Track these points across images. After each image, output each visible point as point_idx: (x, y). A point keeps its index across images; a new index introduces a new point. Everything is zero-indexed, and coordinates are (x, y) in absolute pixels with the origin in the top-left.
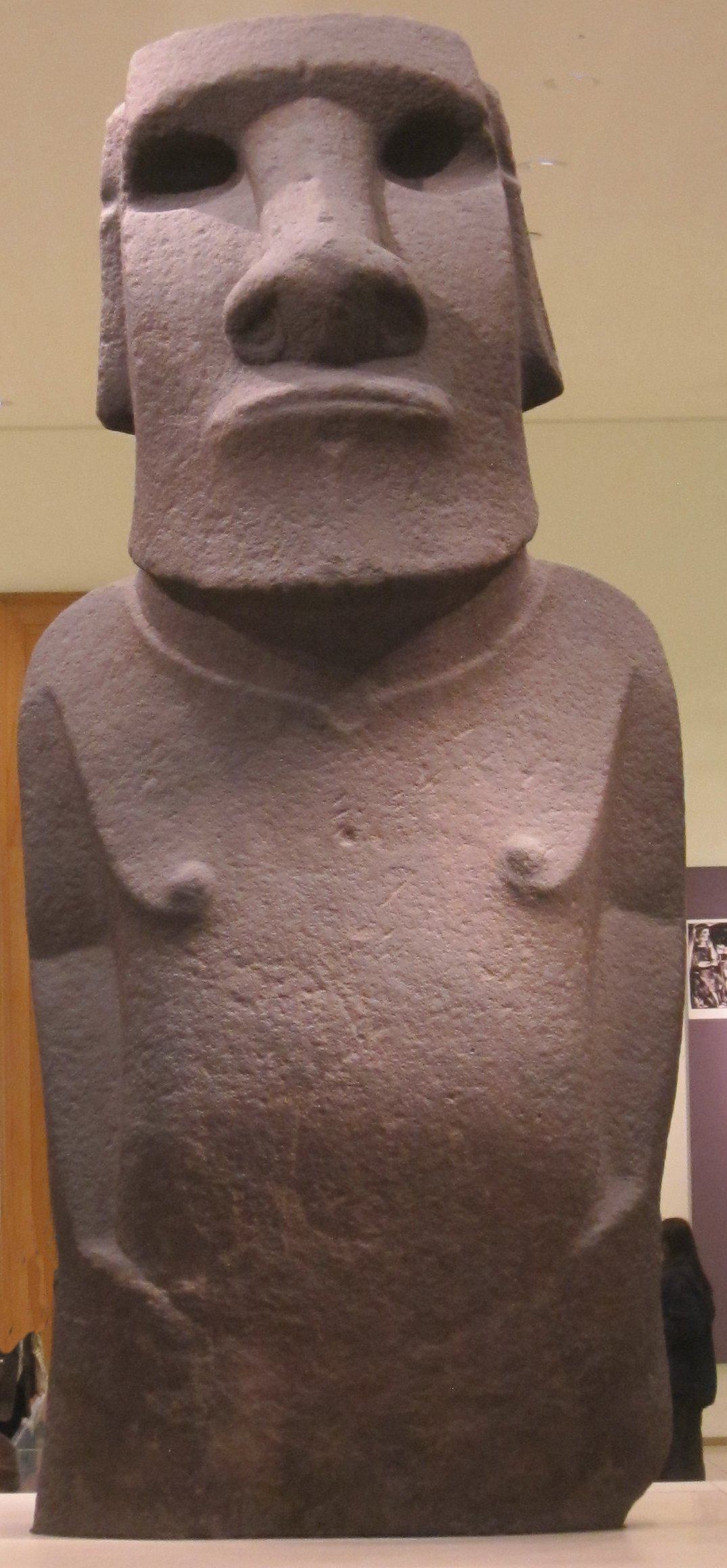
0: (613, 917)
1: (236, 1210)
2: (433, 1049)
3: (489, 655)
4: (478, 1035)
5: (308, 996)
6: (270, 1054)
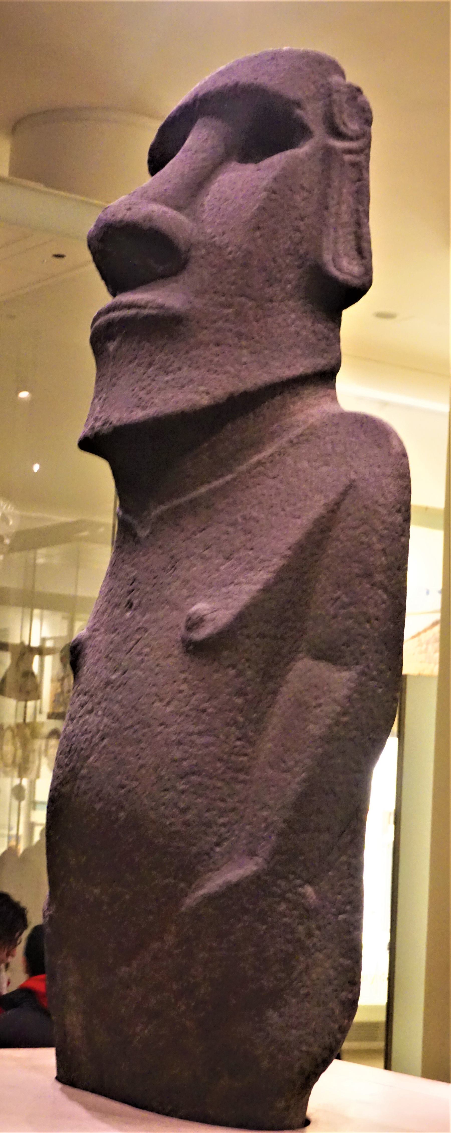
3: (229, 477)
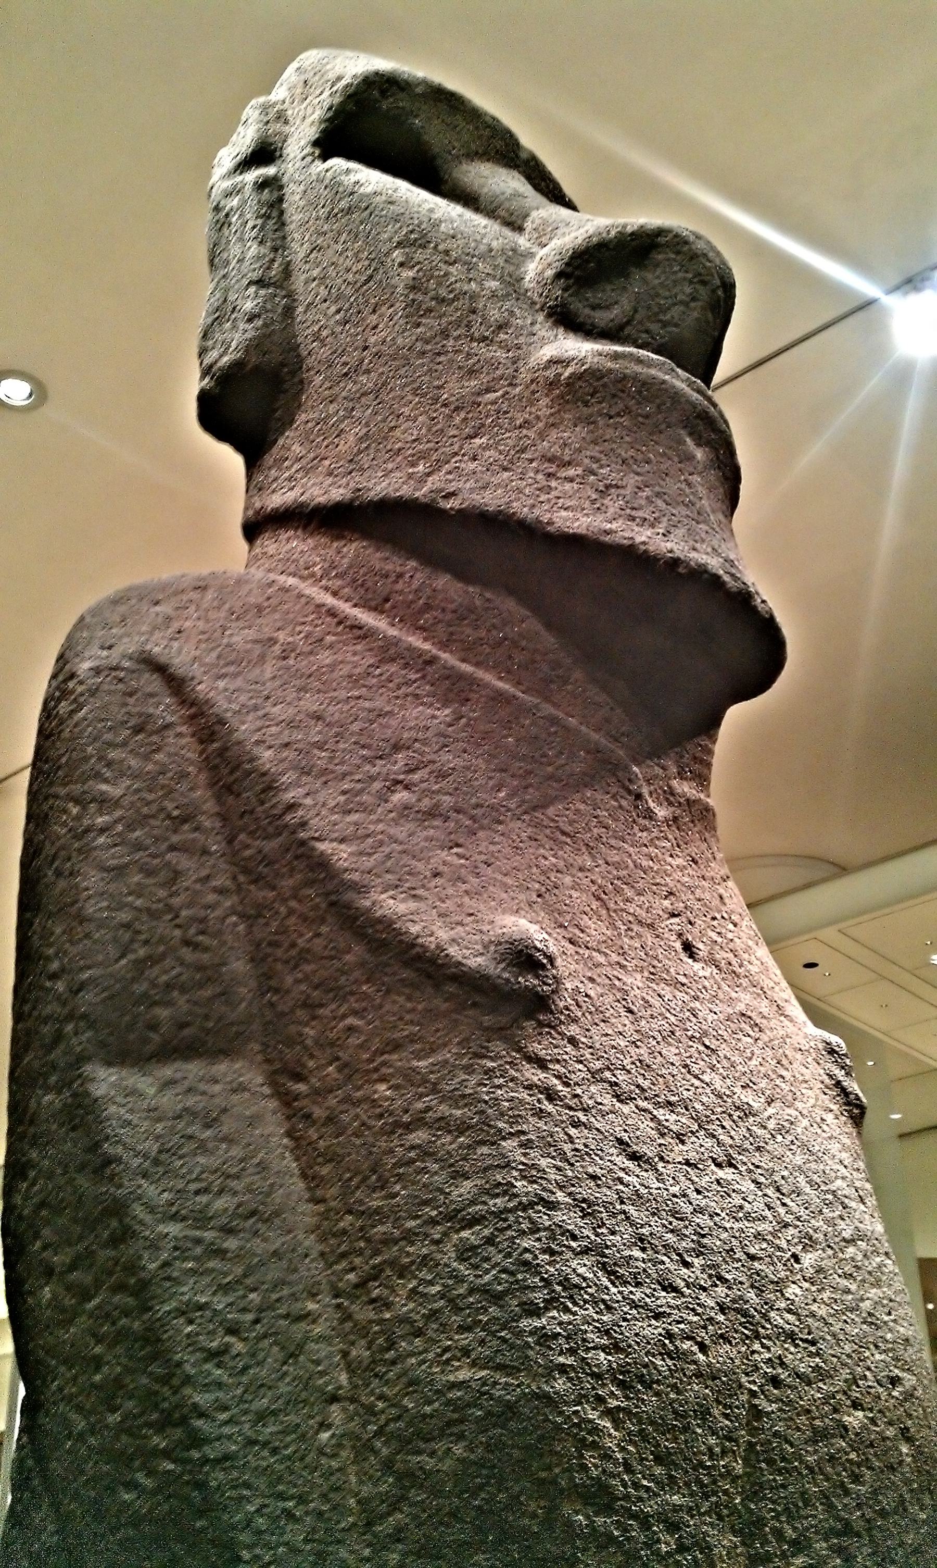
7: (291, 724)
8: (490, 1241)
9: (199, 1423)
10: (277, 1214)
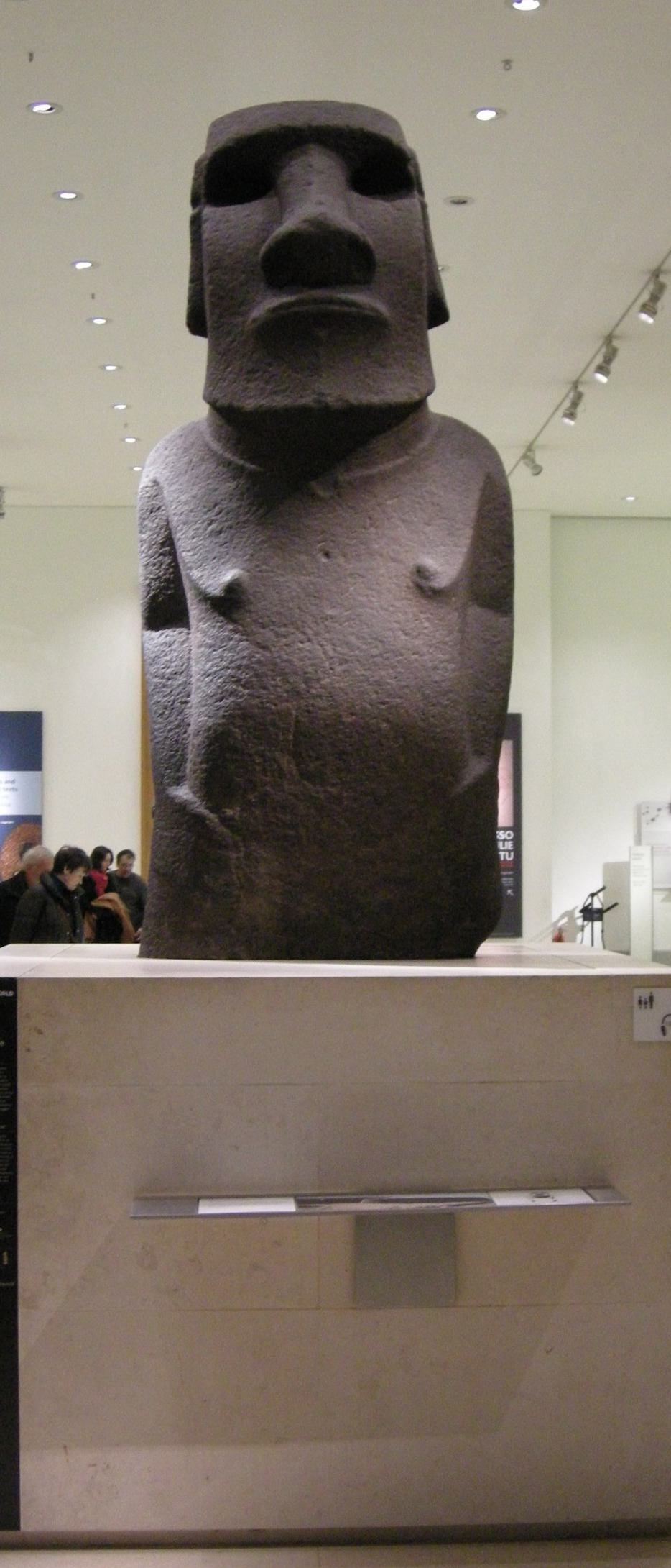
0: (474, 611)
1: (258, 768)
2: (373, 677)
3: (407, 458)
4: (399, 670)
5: (301, 645)
6: (278, 679)
7: (186, 503)
8: (211, 681)
9: (156, 733)
10: (182, 672)
